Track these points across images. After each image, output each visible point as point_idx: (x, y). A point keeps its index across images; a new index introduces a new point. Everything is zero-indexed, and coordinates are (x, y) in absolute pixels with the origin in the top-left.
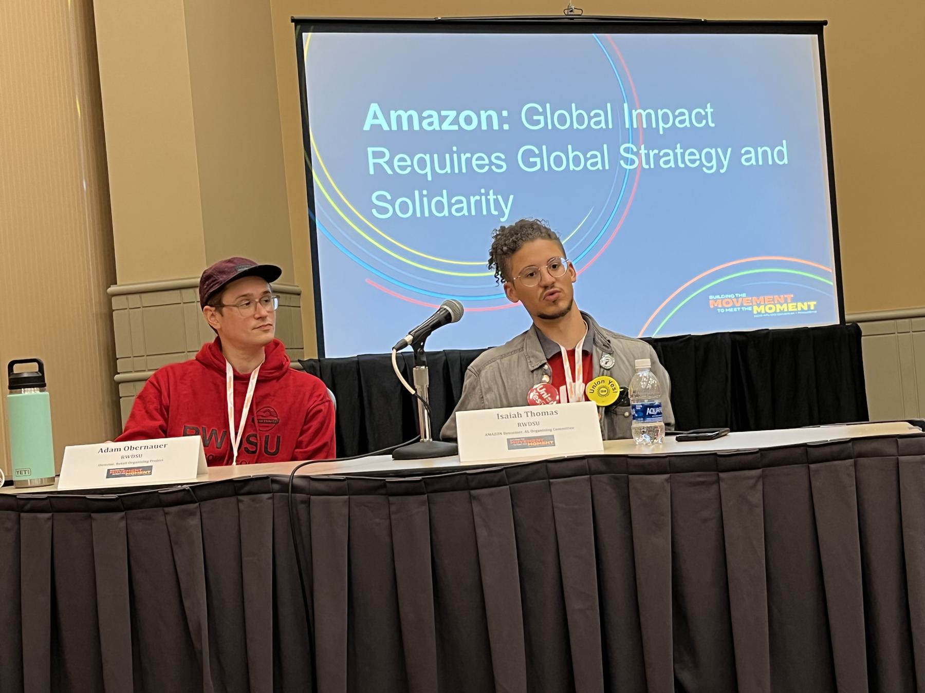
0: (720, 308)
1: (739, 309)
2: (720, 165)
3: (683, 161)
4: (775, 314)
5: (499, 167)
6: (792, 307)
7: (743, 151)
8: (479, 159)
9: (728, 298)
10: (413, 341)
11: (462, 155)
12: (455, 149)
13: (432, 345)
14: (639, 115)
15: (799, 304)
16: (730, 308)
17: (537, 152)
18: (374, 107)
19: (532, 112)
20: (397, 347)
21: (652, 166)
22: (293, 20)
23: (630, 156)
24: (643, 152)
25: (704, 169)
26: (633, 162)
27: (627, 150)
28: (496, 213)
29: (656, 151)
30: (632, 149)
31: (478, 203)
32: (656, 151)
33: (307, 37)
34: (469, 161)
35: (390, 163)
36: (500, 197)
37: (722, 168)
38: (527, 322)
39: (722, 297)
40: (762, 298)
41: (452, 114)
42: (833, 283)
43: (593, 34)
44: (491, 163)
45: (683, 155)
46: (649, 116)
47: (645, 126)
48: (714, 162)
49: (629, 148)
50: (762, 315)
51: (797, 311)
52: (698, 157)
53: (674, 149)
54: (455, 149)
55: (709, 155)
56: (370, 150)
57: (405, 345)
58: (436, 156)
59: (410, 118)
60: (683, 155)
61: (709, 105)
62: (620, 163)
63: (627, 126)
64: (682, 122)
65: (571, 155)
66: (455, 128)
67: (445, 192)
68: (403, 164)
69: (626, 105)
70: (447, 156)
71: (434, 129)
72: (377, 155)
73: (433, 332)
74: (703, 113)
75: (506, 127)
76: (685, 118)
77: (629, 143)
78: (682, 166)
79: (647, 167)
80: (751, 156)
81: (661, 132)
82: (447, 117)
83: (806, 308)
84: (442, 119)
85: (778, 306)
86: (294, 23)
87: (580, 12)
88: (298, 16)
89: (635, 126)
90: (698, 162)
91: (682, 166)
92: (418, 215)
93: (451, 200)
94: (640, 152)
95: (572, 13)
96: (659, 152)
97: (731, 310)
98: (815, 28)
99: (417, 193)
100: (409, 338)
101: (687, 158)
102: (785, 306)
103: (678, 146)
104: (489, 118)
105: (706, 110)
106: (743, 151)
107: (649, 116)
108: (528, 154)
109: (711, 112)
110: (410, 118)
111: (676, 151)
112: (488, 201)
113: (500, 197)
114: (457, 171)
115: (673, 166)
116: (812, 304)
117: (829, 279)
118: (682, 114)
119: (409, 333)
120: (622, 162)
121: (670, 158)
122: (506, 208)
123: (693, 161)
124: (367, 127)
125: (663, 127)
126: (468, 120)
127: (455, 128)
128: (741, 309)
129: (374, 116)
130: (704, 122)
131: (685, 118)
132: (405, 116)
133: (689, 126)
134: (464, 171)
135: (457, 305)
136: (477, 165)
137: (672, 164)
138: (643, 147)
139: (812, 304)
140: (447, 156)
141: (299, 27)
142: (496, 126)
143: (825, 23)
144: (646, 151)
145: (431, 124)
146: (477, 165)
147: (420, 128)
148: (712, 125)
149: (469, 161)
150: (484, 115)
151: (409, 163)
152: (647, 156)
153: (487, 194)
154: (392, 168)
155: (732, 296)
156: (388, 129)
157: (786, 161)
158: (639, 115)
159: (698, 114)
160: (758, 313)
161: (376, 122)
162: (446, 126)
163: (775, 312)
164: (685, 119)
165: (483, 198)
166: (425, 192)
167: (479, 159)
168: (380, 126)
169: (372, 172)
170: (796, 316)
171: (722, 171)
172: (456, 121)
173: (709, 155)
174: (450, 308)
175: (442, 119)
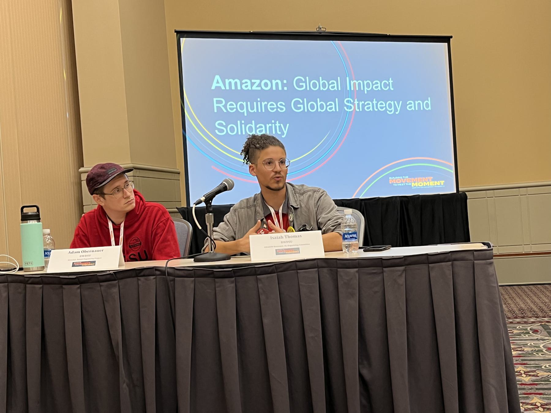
0: (395, 184)
1: (404, 184)
2: (396, 110)
3: (377, 108)
4: (423, 187)
5: (282, 109)
6: (432, 184)
7: (408, 103)
8: (272, 105)
9: (399, 178)
10: (205, 200)
11: (263, 103)
12: (259, 99)
13: (215, 202)
14: (355, 84)
15: (436, 182)
16: (400, 183)
17: (301, 102)
18: (217, 77)
19: (299, 81)
20: (196, 203)
21: (361, 110)
22: (176, 31)
23: (349, 104)
24: (356, 102)
25: (388, 112)
26: (351, 108)
27: (348, 101)
28: (280, 133)
29: (363, 102)
30: (350, 101)
31: (271, 128)
32: (363, 102)
33: (183, 40)
34: (266, 106)
35: (225, 106)
36: (282, 125)
37: (397, 112)
38: (258, 190)
39: (396, 178)
40: (416, 178)
41: (258, 82)
42: (453, 172)
43: (331, 41)
44: (278, 107)
45: (377, 104)
46: (359, 84)
47: (357, 89)
48: (393, 108)
49: (349, 100)
50: (416, 188)
51: (435, 186)
52: (384, 105)
53: (372, 101)
54: (259, 99)
55: (390, 105)
56: (215, 99)
57: (200, 202)
58: (249, 103)
59: (236, 83)
60: (377, 104)
61: (390, 79)
62: (344, 108)
63: (348, 89)
64: (377, 87)
65: (319, 104)
66: (259, 88)
67: (253, 122)
68: (232, 107)
69: (348, 78)
70: (255, 103)
71: (248, 89)
72: (219, 102)
73: (216, 196)
74: (388, 83)
75: (285, 88)
76: (378, 85)
77: (349, 98)
78: (376, 110)
79: (358, 110)
80: (412, 106)
81: (366, 92)
82: (255, 83)
83: (439, 184)
84: (252, 84)
85: (425, 183)
86: (176, 33)
87: (324, 30)
88: (178, 29)
89: (352, 89)
90: (384, 108)
91: (376, 110)
92: (240, 133)
93: (257, 126)
94: (355, 102)
95: (320, 30)
96: (364, 103)
97: (400, 185)
98: (446, 39)
99: (239, 122)
100: (203, 199)
101: (379, 106)
102: (428, 183)
103: (374, 100)
104: (277, 84)
105: (389, 81)
106: (408, 103)
107: (359, 84)
108: (297, 103)
109: (392, 83)
110: (236, 83)
111: (373, 102)
112: (276, 127)
113: (282, 125)
114: (260, 111)
115: (372, 110)
116: (442, 182)
117: (451, 169)
118: (377, 83)
119: (204, 196)
120: (345, 108)
121: (371, 106)
122: (285, 130)
123: (382, 108)
124: (213, 88)
125: (367, 90)
126: (266, 85)
127: (259, 88)
128: (405, 184)
129: (217, 82)
130: (388, 87)
131: (378, 85)
132: (233, 82)
133: (380, 89)
134: (263, 111)
135: (231, 182)
136: (270, 108)
137: (371, 109)
138: (356, 100)
139: (442, 182)
140: (255, 103)
141: (178, 35)
142: (280, 88)
143: (451, 37)
144: (358, 102)
145: (246, 86)
146: (270, 108)
147: (241, 89)
148: (392, 89)
149: (266, 106)
150: (274, 82)
151: (235, 106)
152: (358, 104)
153: (275, 123)
154: (226, 109)
155: (401, 178)
156: (224, 89)
157: (430, 108)
158: (355, 84)
159: (385, 83)
160: (414, 187)
161: (218, 85)
162: (254, 88)
163: (423, 186)
164: (335, 86)
165: (273, 125)
166: (243, 122)
167: (272, 105)
168: (220, 87)
169: (216, 111)
170: (434, 188)
171: (397, 113)
172: (259, 85)
173: (390, 105)
174: (227, 183)
175: (252, 84)
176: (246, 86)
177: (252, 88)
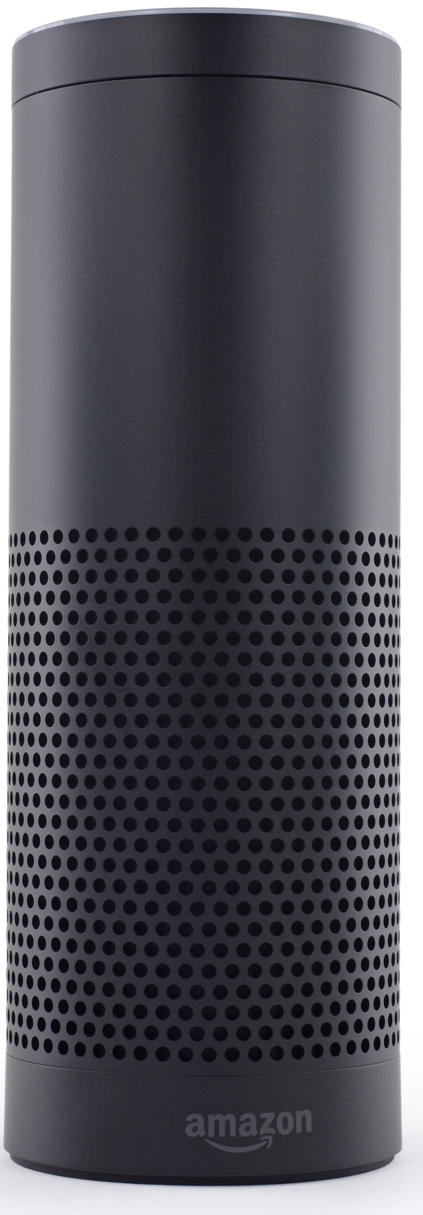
41: (269, 1117)
59: (227, 1123)
66: (273, 1131)
82: (265, 1119)
84: (260, 1123)
104: (304, 1119)
110: (227, 1123)
127: (273, 1131)
145: (248, 1129)
150: (299, 1114)
172: (273, 1125)
175: (260, 1123)
177: (259, 1132)
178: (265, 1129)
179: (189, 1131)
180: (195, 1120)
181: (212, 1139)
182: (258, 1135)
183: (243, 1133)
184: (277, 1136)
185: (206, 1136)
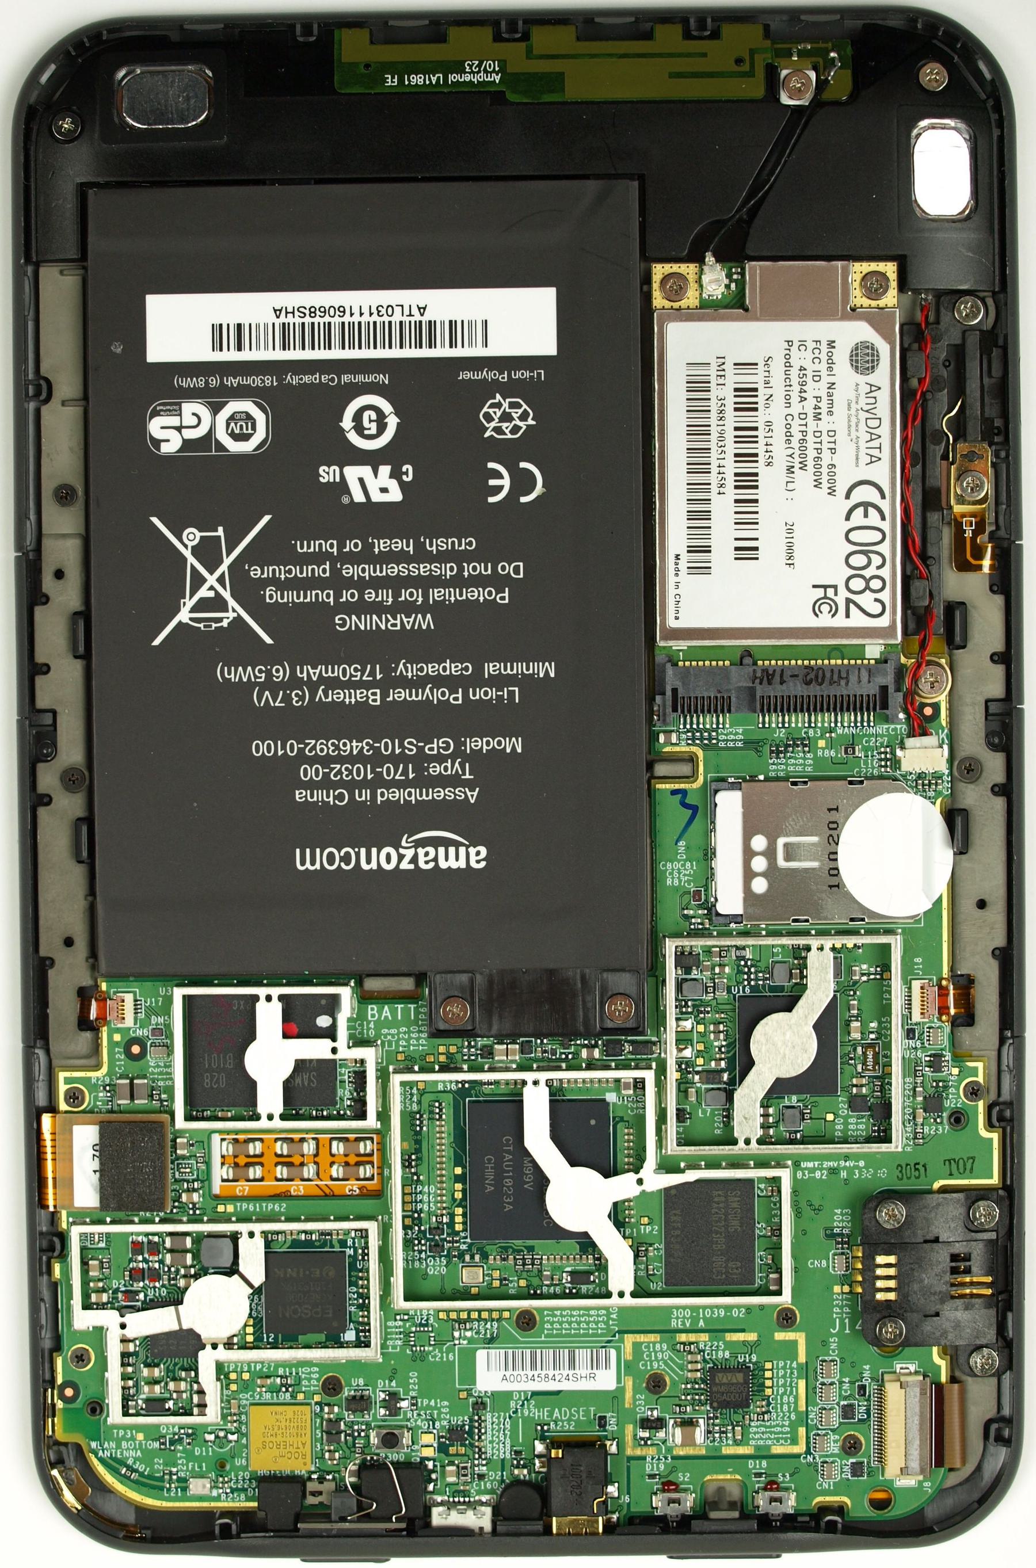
41: (405, 865)
59: (447, 859)
66: (401, 851)
82: (409, 863)
84: (414, 860)
104: (369, 861)
110: (447, 859)
127: (401, 851)
132: (453, 864)
145: (427, 854)
150: (374, 865)
172: (401, 857)
175: (414, 860)
176: (427, 854)
178: (409, 854)
179: (483, 851)
180: (478, 862)
181: (463, 845)
182: (416, 847)
183: (431, 850)
184: (397, 846)
185: (467, 847)
